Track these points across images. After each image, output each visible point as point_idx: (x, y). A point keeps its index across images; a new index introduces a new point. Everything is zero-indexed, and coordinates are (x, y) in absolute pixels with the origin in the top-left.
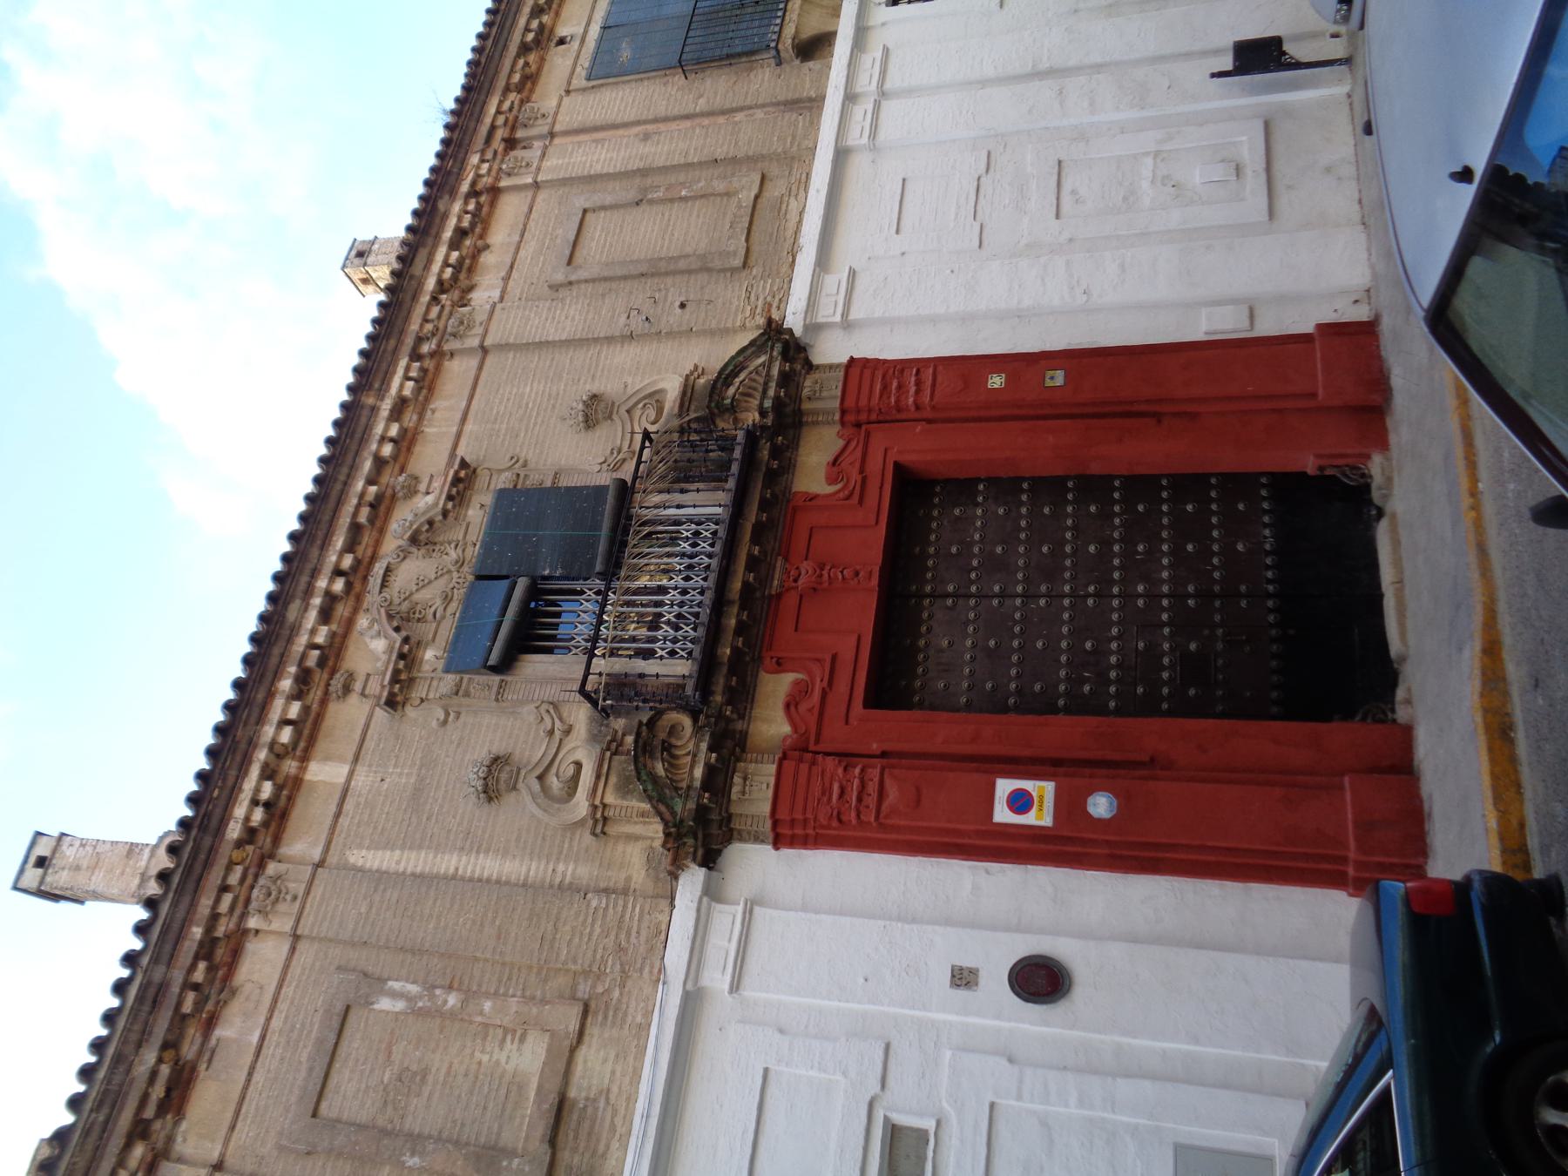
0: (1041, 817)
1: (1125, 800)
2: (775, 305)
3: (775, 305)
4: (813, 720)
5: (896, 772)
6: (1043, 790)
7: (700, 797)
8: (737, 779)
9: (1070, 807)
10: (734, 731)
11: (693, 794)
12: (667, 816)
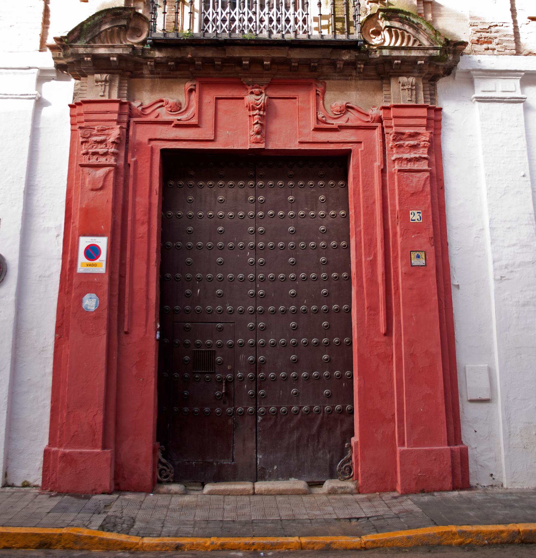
0: (83, 265)
1: (96, 315)
2: (490, 46)
3: (490, 46)
4: (152, 118)
5: (112, 175)
6: (100, 266)
7: (88, 55)
8: (104, 76)
9: (89, 283)
10: (142, 69)
11: (89, 50)
12: (71, 38)
